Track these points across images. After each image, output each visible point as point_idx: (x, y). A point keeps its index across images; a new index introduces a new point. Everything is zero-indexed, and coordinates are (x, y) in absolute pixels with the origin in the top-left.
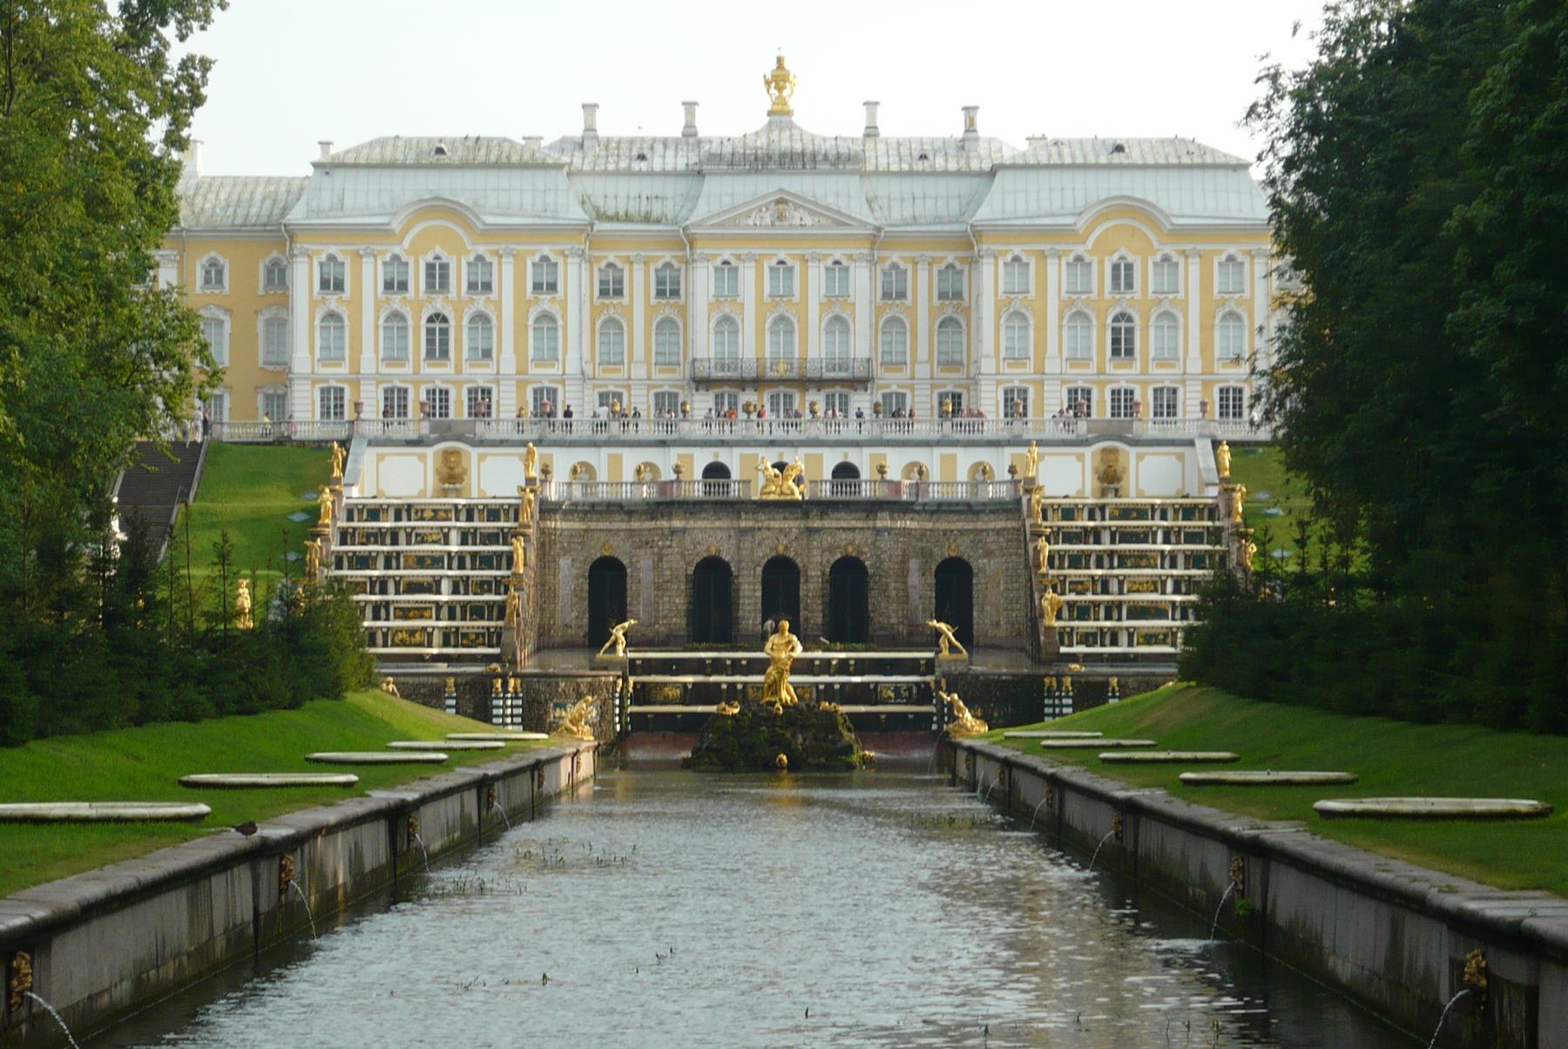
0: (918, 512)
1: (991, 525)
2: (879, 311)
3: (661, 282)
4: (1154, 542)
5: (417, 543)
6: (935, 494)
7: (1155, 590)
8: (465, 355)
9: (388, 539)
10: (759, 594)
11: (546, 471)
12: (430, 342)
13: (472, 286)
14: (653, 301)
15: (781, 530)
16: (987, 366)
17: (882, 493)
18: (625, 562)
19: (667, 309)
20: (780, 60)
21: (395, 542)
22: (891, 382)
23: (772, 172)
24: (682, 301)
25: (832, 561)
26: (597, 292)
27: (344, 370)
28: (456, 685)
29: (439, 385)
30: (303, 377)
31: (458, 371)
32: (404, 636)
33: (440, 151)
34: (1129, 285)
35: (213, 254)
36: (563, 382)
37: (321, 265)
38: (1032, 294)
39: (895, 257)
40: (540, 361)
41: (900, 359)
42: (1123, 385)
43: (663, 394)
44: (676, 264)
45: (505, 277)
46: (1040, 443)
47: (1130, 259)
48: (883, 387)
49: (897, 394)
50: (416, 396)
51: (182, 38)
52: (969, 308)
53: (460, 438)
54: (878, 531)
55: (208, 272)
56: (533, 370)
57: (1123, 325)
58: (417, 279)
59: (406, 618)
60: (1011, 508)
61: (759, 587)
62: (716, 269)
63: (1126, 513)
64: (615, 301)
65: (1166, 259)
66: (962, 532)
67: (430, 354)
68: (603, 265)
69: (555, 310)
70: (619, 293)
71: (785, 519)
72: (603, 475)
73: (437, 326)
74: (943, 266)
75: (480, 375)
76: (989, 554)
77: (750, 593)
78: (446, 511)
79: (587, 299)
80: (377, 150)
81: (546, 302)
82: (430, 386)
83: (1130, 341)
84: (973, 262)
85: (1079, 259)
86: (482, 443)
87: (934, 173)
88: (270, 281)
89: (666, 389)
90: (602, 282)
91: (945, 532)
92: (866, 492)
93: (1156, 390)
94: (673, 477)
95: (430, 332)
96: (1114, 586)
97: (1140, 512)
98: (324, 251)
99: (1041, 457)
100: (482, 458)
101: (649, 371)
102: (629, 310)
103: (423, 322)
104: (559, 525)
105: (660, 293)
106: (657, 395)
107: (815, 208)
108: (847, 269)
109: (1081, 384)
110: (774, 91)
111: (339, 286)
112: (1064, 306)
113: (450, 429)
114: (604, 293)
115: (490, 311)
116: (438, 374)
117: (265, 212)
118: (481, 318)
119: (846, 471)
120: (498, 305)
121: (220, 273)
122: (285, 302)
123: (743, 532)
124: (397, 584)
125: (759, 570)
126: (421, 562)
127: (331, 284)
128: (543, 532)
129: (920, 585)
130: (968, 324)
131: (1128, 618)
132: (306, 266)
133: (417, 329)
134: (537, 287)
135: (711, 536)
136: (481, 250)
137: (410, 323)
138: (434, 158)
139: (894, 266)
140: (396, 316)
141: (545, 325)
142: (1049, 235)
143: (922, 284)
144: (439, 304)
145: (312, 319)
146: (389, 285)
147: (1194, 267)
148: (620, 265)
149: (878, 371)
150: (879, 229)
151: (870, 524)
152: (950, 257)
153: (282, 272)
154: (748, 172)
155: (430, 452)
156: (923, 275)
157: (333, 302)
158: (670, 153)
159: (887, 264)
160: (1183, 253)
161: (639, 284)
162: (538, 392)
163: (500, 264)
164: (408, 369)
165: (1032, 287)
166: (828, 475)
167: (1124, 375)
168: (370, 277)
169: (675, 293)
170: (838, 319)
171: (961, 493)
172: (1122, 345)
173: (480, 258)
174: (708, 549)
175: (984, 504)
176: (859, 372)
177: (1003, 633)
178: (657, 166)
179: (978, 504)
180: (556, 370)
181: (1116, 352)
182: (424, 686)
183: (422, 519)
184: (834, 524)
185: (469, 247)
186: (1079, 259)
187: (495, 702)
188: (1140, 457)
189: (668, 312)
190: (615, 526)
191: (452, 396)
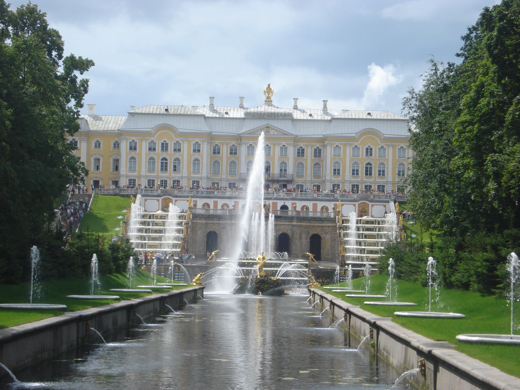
0: (305, 220)
1: (327, 225)
2: (295, 160)
3: (231, 150)
4: (376, 231)
5: (156, 226)
6: (311, 215)
7: (375, 246)
9: (147, 224)
11: (195, 205)
12: (162, 166)
13: (175, 150)
14: (229, 156)
16: (328, 178)
17: (294, 214)
18: (218, 233)
19: (233, 158)
20: (269, 85)
21: (149, 225)
22: (299, 181)
23: (265, 119)
24: (237, 156)
26: (212, 153)
27: (136, 174)
29: (164, 179)
30: (123, 176)
31: (170, 174)
34: (371, 155)
35: (98, 138)
36: (201, 179)
37: (130, 143)
38: (342, 156)
39: (301, 145)
40: (194, 173)
42: (368, 184)
43: (231, 183)
44: (236, 145)
45: (185, 147)
46: (342, 201)
47: (371, 147)
48: (296, 183)
49: (301, 185)
50: (157, 183)
51: (82, 73)
53: (170, 195)
54: (293, 226)
55: (96, 144)
56: (193, 175)
57: (369, 166)
58: (159, 147)
59: (151, 248)
60: (333, 220)
62: (248, 147)
63: (367, 222)
64: (218, 155)
65: (382, 147)
66: (318, 226)
67: (162, 169)
68: (214, 145)
70: (219, 153)
72: (212, 207)
73: (164, 161)
74: (315, 148)
75: (176, 176)
76: (326, 233)
78: (164, 216)
79: (209, 155)
80: (148, 109)
81: (196, 155)
82: (162, 179)
83: (371, 171)
84: (325, 146)
85: (356, 146)
86: (176, 197)
87: (314, 120)
88: (115, 147)
89: (232, 182)
90: (214, 150)
91: (313, 226)
92: (290, 214)
93: (378, 186)
94: (233, 208)
95: (162, 163)
96: (363, 244)
97: (372, 222)
98: (131, 139)
99: (343, 205)
100: (176, 201)
101: (227, 176)
102: (222, 158)
103: (160, 160)
104: (198, 221)
105: (231, 153)
106: (229, 184)
107: (278, 130)
108: (287, 148)
109: (355, 183)
110: (267, 95)
111: (135, 149)
113: (167, 192)
114: (214, 153)
115: (180, 158)
116: (164, 175)
117: (114, 127)
118: (177, 159)
119: (284, 208)
120: (183, 155)
121: (99, 144)
122: (119, 154)
124: (149, 238)
126: (156, 231)
127: (133, 148)
128: (193, 223)
129: (306, 242)
131: (367, 254)
132: (125, 143)
134: (194, 151)
136: (178, 139)
137: (156, 160)
138: (165, 112)
139: (301, 147)
140: (152, 158)
141: (196, 162)
142: (347, 140)
144: (164, 155)
145: (127, 159)
146: (150, 149)
147: (391, 150)
149: (295, 178)
150: (296, 136)
151: (291, 223)
152: (318, 145)
153: (118, 144)
154: (258, 119)
155: (160, 199)
157: (133, 154)
158: (235, 112)
159: (299, 147)
161: (225, 151)
162: (194, 182)
163: (183, 144)
164: (155, 174)
165: (342, 155)
166: (279, 208)
167: (369, 181)
169: (235, 153)
170: (284, 163)
171: (318, 215)
172: (368, 172)
173: (177, 142)
175: (325, 218)
176: (290, 179)
177: (330, 257)
178: (231, 116)
179: (323, 218)
180: (199, 176)
181: (366, 174)
183: (157, 219)
184: (280, 223)
185: (174, 138)
188: (372, 206)
189: (233, 159)
190: (215, 222)
191: (168, 182)
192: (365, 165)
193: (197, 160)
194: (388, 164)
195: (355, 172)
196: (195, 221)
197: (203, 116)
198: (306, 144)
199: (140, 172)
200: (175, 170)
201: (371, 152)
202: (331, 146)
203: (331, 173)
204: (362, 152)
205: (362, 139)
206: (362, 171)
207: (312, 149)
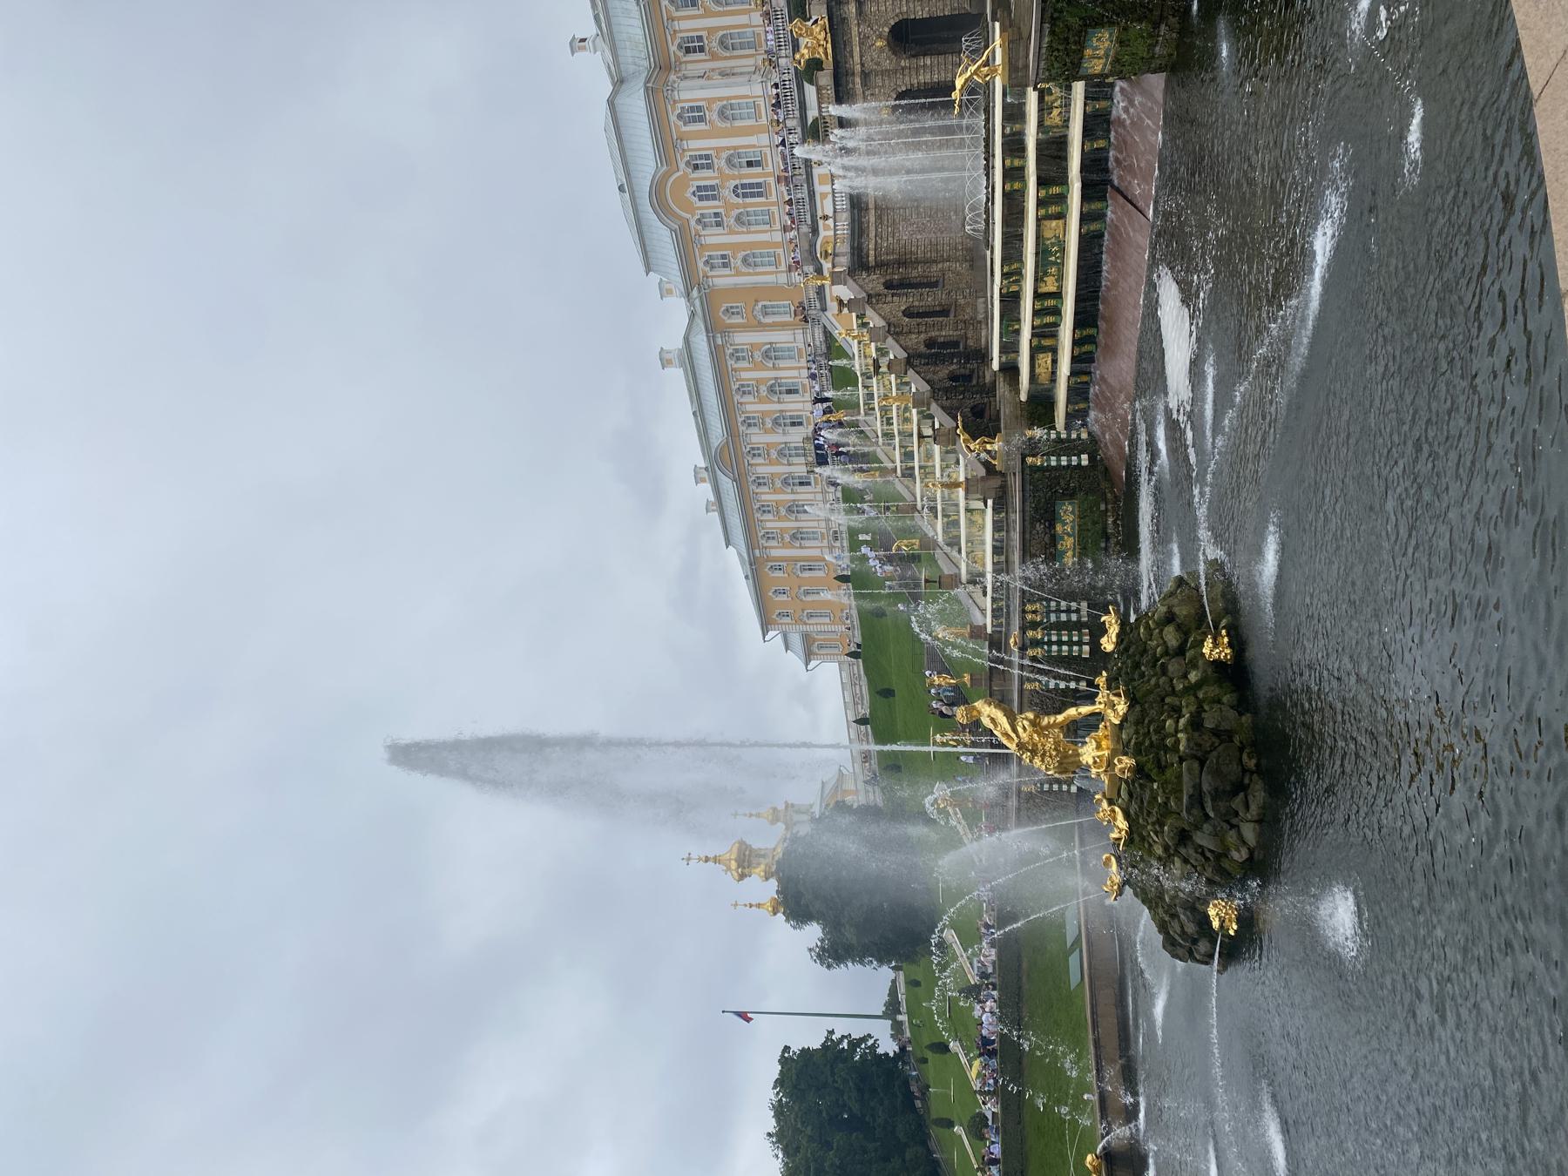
8: (759, 170)
12: (753, 195)
15: (861, 44)
31: (768, 175)
32: (974, 530)
33: (621, 189)
40: (757, 116)
45: (696, 145)
53: (813, 245)
56: (764, 121)
58: (709, 207)
67: (760, 195)
68: (680, 54)
69: (716, 106)
70: (700, 38)
81: (712, 116)
95: (745, 195)
103: (740, 200)
104: (872, 246)
114: (701, 49)
115: (724, 155)
118: (729, 161)
133: (745, 205)
136: (682, 166)
140: (738, 219)
144: (727, 193)
145: (749, 274)
148: (677, 41)
157: (737, 262)
168: (714, 237)
193: (722, 114)
196: (871, 258)
197: (611, 103)
199: (776, 245)
200: (758, 164)
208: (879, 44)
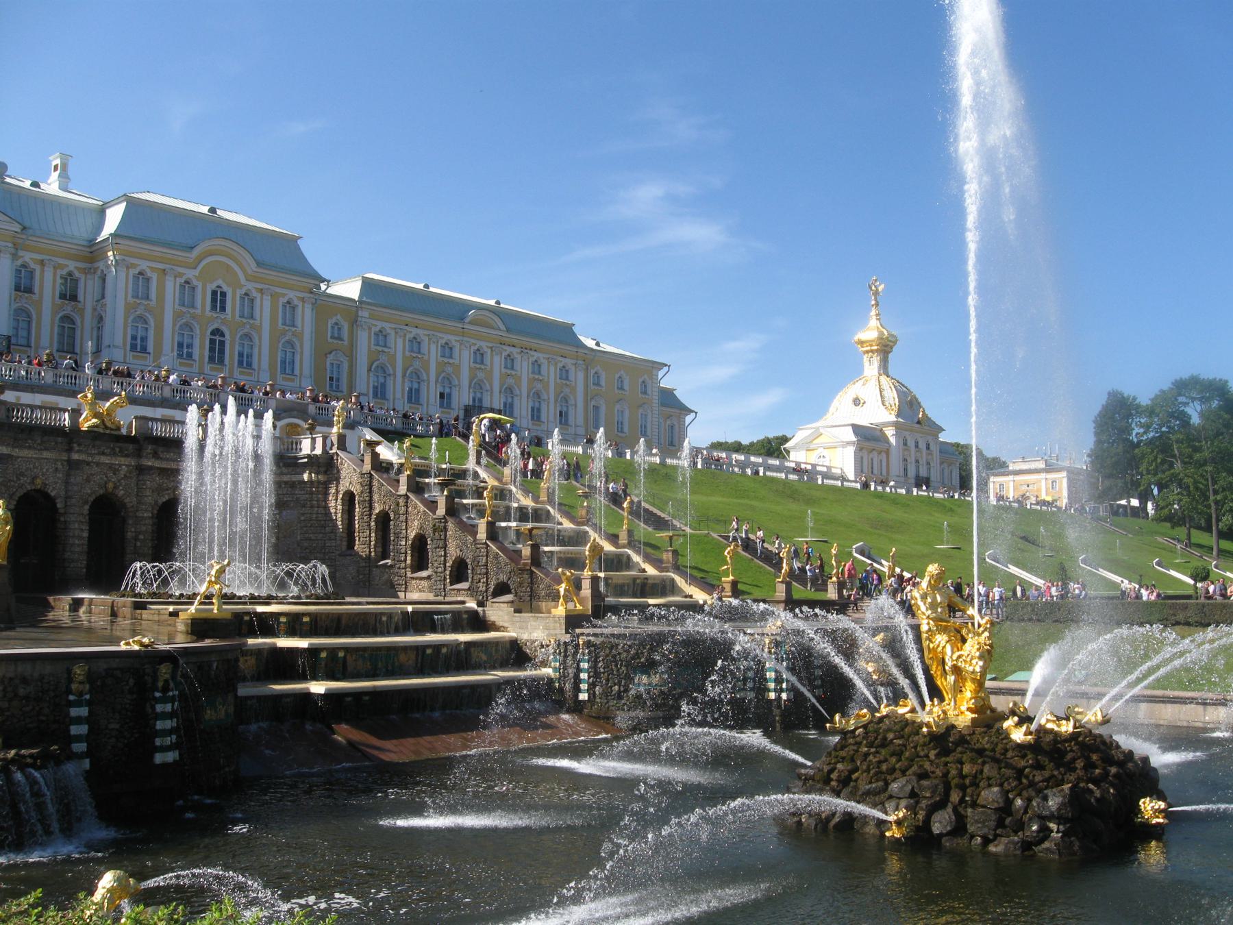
10: (86, 534)
15: (111, 467)
25: (160, 502)
28: (90, 677)
34: (223, 309)
38: (153, 303)
39: (28, 257)
41: (23, 342)
47: (225, 288)
52: (83, 309)
57: (218, 338)
61: (85, 527)
71: (114, 454)
74: (64, 272)
77: (77, 531)
83: (222, 352)
112: (177, 316)
123: (72, 465)
125: (87, 507)
130: (82, 322)
135: (43, 468)
139: (24, 266)
143: (48, 285)
152: (72, 265)
156: (49, 275)
159: (19, 262)
160: (261, 291)
165: (153, 295)
174: (32, 482)
181: (211, 359)
182: (25, 681)
186: (187, 282)
187: (159, 708)
192: (208, 336)
194: (260, 338)
195: (184, 351)
198: (39, 257)
201: (223, 302)
202: (128, 268)
203: (125, 344)
204: (203, 299)
205: (204, 263)
206: (200, 349)
207: (55, 274)
208: (110, 486)
